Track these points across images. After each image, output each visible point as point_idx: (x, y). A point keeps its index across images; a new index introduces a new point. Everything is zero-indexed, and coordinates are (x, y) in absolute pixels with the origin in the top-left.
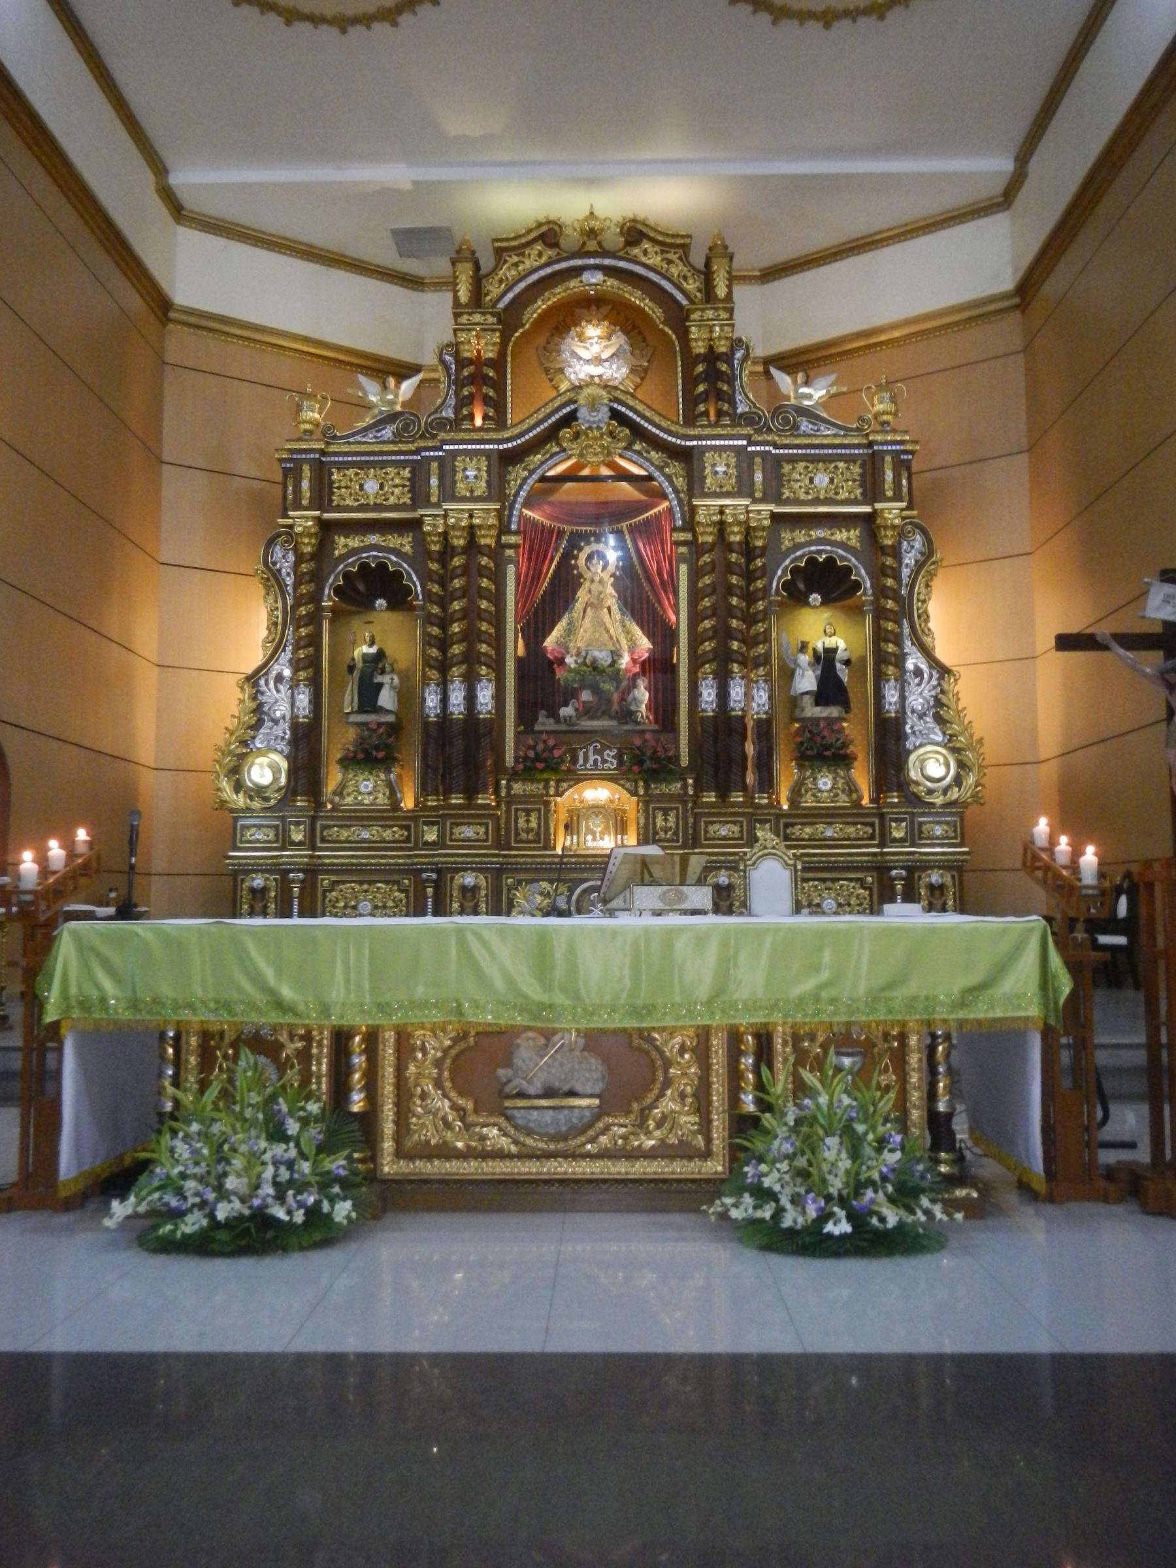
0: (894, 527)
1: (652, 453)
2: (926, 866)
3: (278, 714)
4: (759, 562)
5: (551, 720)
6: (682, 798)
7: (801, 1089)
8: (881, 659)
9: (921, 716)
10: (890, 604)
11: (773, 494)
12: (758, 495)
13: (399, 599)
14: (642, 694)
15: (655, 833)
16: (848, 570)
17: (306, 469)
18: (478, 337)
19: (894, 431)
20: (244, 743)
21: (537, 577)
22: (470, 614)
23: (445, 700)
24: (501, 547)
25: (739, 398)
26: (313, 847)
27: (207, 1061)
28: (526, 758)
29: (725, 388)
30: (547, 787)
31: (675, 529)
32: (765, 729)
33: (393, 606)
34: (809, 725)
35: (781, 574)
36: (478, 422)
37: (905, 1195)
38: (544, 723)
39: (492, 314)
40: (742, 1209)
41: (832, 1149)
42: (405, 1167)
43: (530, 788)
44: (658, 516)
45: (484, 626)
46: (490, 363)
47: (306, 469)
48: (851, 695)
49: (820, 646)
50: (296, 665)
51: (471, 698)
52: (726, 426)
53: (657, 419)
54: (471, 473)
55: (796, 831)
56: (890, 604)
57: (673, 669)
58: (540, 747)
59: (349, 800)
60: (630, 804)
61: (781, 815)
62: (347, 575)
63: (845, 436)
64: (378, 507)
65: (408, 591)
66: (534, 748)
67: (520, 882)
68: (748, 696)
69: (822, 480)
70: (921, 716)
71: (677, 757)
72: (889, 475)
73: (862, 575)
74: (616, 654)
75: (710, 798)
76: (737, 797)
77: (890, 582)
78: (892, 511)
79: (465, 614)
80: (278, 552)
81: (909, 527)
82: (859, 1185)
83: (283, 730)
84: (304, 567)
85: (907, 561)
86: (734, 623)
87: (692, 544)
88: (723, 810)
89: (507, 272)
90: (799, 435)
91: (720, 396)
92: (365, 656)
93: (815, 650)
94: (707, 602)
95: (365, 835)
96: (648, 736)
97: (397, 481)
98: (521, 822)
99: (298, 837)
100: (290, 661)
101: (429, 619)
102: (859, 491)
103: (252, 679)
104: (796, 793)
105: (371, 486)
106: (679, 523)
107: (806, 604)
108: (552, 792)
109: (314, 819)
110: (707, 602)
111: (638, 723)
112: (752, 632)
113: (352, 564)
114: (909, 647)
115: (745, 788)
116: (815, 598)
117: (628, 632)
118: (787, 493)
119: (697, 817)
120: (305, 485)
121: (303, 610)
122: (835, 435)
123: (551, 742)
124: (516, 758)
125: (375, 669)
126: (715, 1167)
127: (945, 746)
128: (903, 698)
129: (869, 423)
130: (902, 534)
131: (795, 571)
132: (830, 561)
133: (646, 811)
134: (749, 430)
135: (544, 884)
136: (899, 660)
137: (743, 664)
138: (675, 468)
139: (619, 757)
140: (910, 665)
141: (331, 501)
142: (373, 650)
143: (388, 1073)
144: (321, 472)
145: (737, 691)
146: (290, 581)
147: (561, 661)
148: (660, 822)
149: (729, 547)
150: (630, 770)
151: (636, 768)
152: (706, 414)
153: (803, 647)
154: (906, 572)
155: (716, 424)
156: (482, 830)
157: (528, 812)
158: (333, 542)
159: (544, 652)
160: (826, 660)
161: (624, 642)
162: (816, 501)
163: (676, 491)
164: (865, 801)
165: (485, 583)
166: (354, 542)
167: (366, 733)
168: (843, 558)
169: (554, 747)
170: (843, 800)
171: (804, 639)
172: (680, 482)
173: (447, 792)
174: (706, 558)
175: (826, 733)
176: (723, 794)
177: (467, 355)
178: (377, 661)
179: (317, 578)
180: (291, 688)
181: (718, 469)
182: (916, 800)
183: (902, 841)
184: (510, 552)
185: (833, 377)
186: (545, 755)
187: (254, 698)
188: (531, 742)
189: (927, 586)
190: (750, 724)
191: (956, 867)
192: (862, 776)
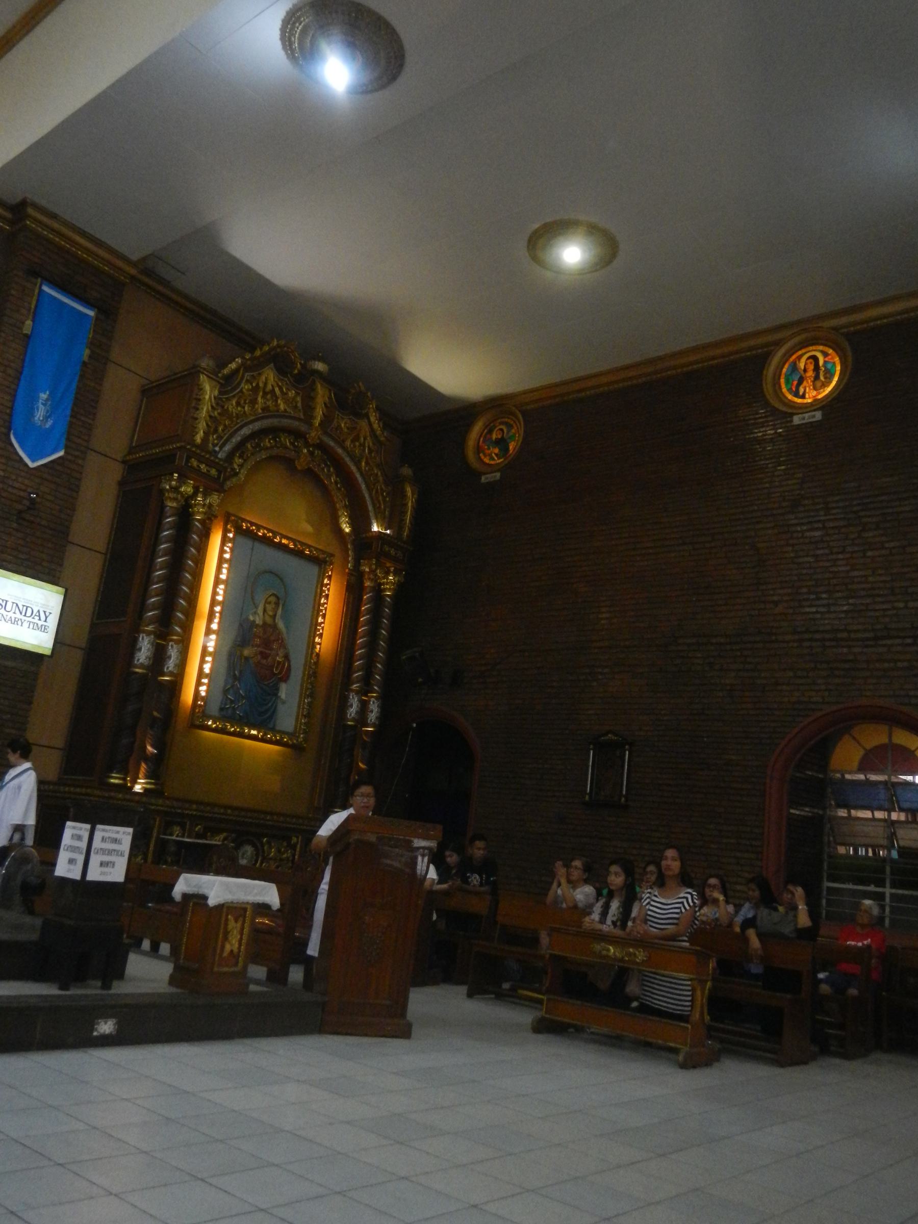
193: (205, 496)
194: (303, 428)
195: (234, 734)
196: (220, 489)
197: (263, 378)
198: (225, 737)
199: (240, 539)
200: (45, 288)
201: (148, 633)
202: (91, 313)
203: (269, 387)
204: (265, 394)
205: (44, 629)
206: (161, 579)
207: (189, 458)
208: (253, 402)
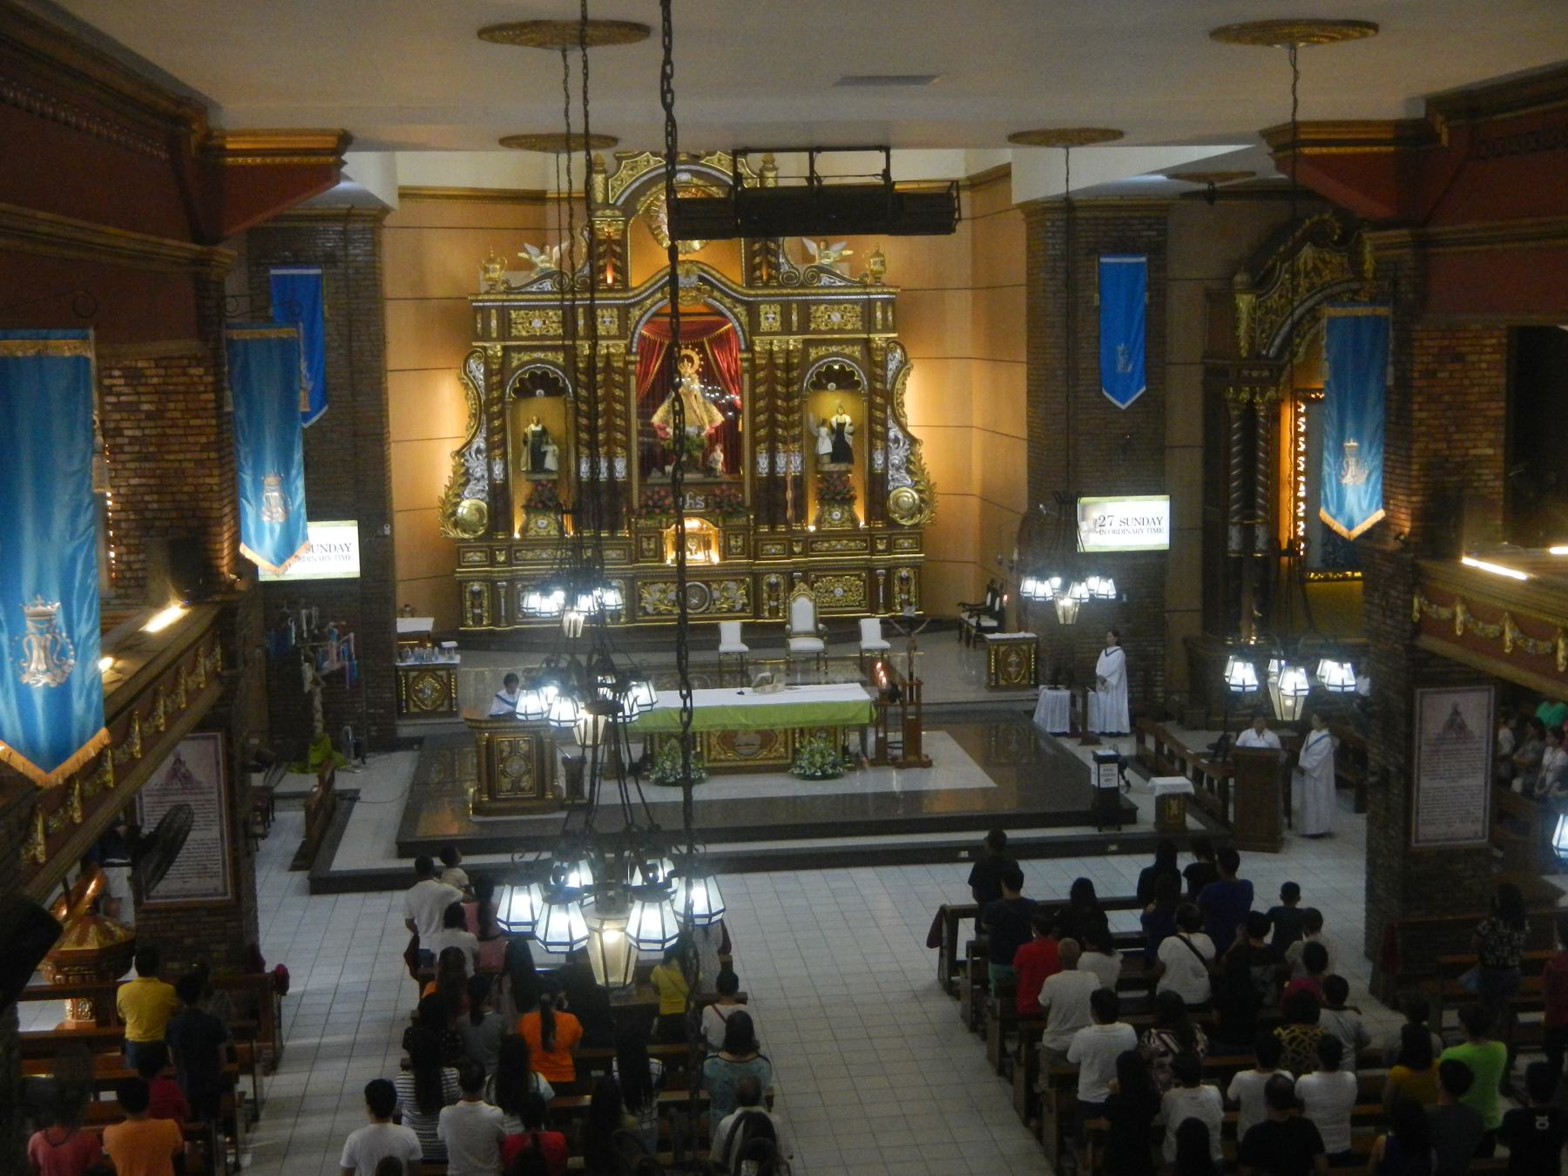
0: (882, 349)
1: (727, 301)
2: (897, 567)
3: (478, 475)
4: (795, 374)
5: (660, 474)
6: (747, 528)
7: (810, 742)
8: (873, 435)
9: (898, 469)
10: (879, 400)
11: (804, 328)
12: (795, 329)
13: (552, 387)
14: (719, 456)
15: (730, 550)
16: (852, 374)
17: (494, 311)
18: (609, 225)
19: (884, 285)
20: (458, 495)
21: (646, 374)
22: (610, 412)
23: (594, 468)
24: (627, 363)
25: (782, 260)
26: (511, 565)
27: (661, 741)
28: (647, 505)
29: (773, 259)
30: (660, 522)
31: (740, 351)
32: (799, 482)
33: (548, 394)
34: (827, 477)
35: (810, 376)
36: (610, 281)
37: (834, 766)
38: (655, 477)
39: (619, 209)
40: (797, 771)
41: (818, 758)
42: (710, 765)
43: (649, 523)
44: (727, 332)
45: (618, 421)
46: (615, 242)
47: (494, 311)
48: (856, 457)
49: (834, 420)
50: (491, 447)
51: (611, 468)
52: (774, 287)
53: (729, 283)
54: (607, 320)
55: (818, 546)
56: (879, 400)
57: (739, 436)
58: (656, 497)
59: (532, 533)
60: (713, 531)
61: (811, 535)
62: (522, 381)
63: (851, 287)
64: (543, 337)
65: (564, 390)
66: (651, 498)
67: (645, 584)
68: (788, 463)
69: (836, 317)
70: (898, 469)
71: (742, 504)
72: (879, 314)
73: (860, 376)
74: (701, 428)
75: (764, 529)
76: (782, 528)
77: (879, 385)
78: (878, 338)
79: (606, 411)
80: (473, 364)
81: (892, 345)
82: (823, 764)
83: (484, 484)
84: (495, 379)
85: (890, 366)
86: (780, 417)
87: (752, 361)
88: (772, 537)
89: (624, 173)
90: (818, 287)
91: (771, 265)
92: (534, 433)
93: (831, 426)
94: (762, 403)
95: (544, 556)
96: (724, 487)
97: (555, 319)
98: (645, 545)
99: (501, 558)
100: (487, 439)
101: (577, 412)
102: (859, 325)
103: (459, 453)
104: (818, 522)
105: (537, 323)
106: (743, 347)
107: (824, 388)
108: (664, 525)
109: (510, 547)
110: (762, 403)
111: (716, 477)
112: (791, 418)
113: (524, 373)
114: (890, 423)
115: (787, 523)
116: (832, 386)
117: (708, 411)
118: (813, 326)
119: (756, 541)
120: (494, 323)
121: (495, 409)
122: (845, 287)
123: (662, 493)
124: (641, 507)
125: (541, 443)
126: (789, 761)
127: (912, 488)
128: (886, 459)
129: (867, 275)
130: (887, 351)
131: (819, 375)
132: (842, 367)
133: (724, 537)
134: (790, 291)
135: (662, 586)
136: (885, 438)
137: (785, 443)
138: (739, 309)
139: (706, 501)
140: (892, 434)
141: (510, 333)
142: (539, 428)
143: (705, 743)
144: (503, 313)
145: (781, 460)
146: (482, 383)
147: (663, 429)
148: (733, 543)
149: (776, 366)
150: (713, 511)
151: (718, 511)
152: (761, 277)
153: (824, 423)
154: (890, 374)
155: (766, 285)
156: (621, 552)
157: (649, 539)
158: (511, 358)
159: (651, 425)
160: (838, 432)
161: (706, 420)
162: (832, 331)
163: (741, 325)
164: (862, 524)
165: (618, 392)
166: (525, 357)
167: (540, 488)
168: (849, 366)
169: (666, 497)
170: (848, 527)
171: (826, 416)
172: (744, 319)
173: (599, 528)
174: (761, 375)
175: (838, 482)
176: (773, 527)
177: (602, 237)
178: (542, 436)
179: (502, 384)
180: (488, 457)
181: (770, 317)
182: (893, 524)
183: (883, 551)
184: (632, 367)
185: (843, 244)
186: (660, 503)
187: (463, 465)
188: (649, 493)
189: (904, 384)
190: (789, 479)
191: (915, 566)
192: (860, 511)
193: (1262, 396)
194: (1355, 286)
195: (1338, 580)
196: (1276, 383)
197: (1302, 260)
198: (1327, 584)
199: (1315, 407)
200: (1103, 260)
201: (1234, 524)
202: (1143, 259)
203: (1310, 265)
204: (1307, 275)
205: (1159, 531)
206: (1238, 477)
207: (1239, 372)
208: (1295, 290)
